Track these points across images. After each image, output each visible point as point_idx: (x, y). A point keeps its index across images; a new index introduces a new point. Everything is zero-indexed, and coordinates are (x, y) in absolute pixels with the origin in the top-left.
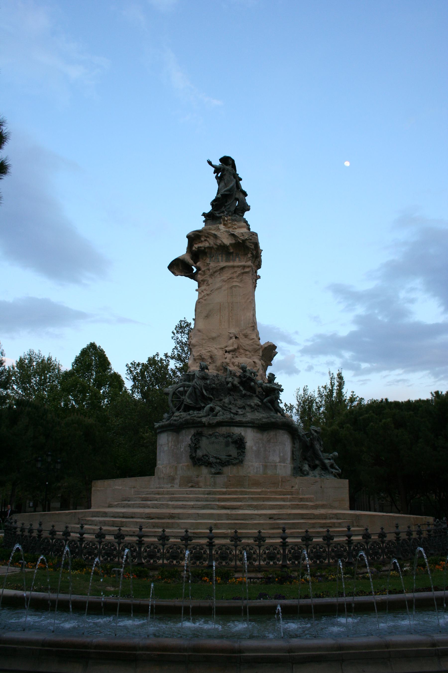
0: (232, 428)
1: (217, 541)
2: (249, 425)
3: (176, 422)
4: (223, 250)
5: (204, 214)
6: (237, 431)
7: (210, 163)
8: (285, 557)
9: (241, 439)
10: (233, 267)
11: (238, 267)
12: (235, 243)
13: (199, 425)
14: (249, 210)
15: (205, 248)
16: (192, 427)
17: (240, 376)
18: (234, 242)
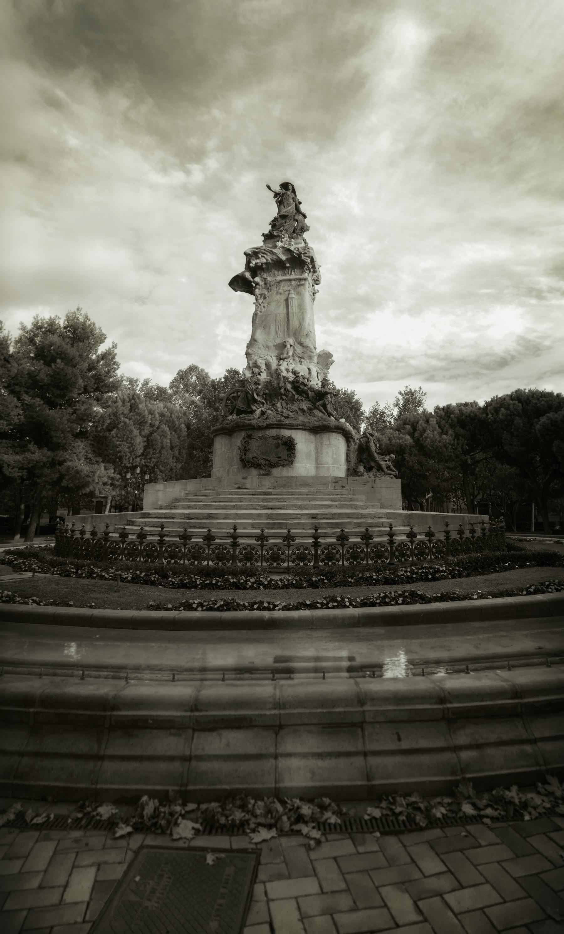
0: (282, 430)
1: (241, 541)
2: (299, 427)
3: (227, 426)
4: (279, 265)
5: (263, 235)
6: (287, 433)
7: (269, 187)
8: (316, 558)
9: (290, 440)
10: (290, 280)
11: (295, 280)
12: (291, 258)
13: (249, 427)
14: (308, 230)
15: (262, 264)
16: (243, 430)
17: (293, 381)
18: (290, 256)
